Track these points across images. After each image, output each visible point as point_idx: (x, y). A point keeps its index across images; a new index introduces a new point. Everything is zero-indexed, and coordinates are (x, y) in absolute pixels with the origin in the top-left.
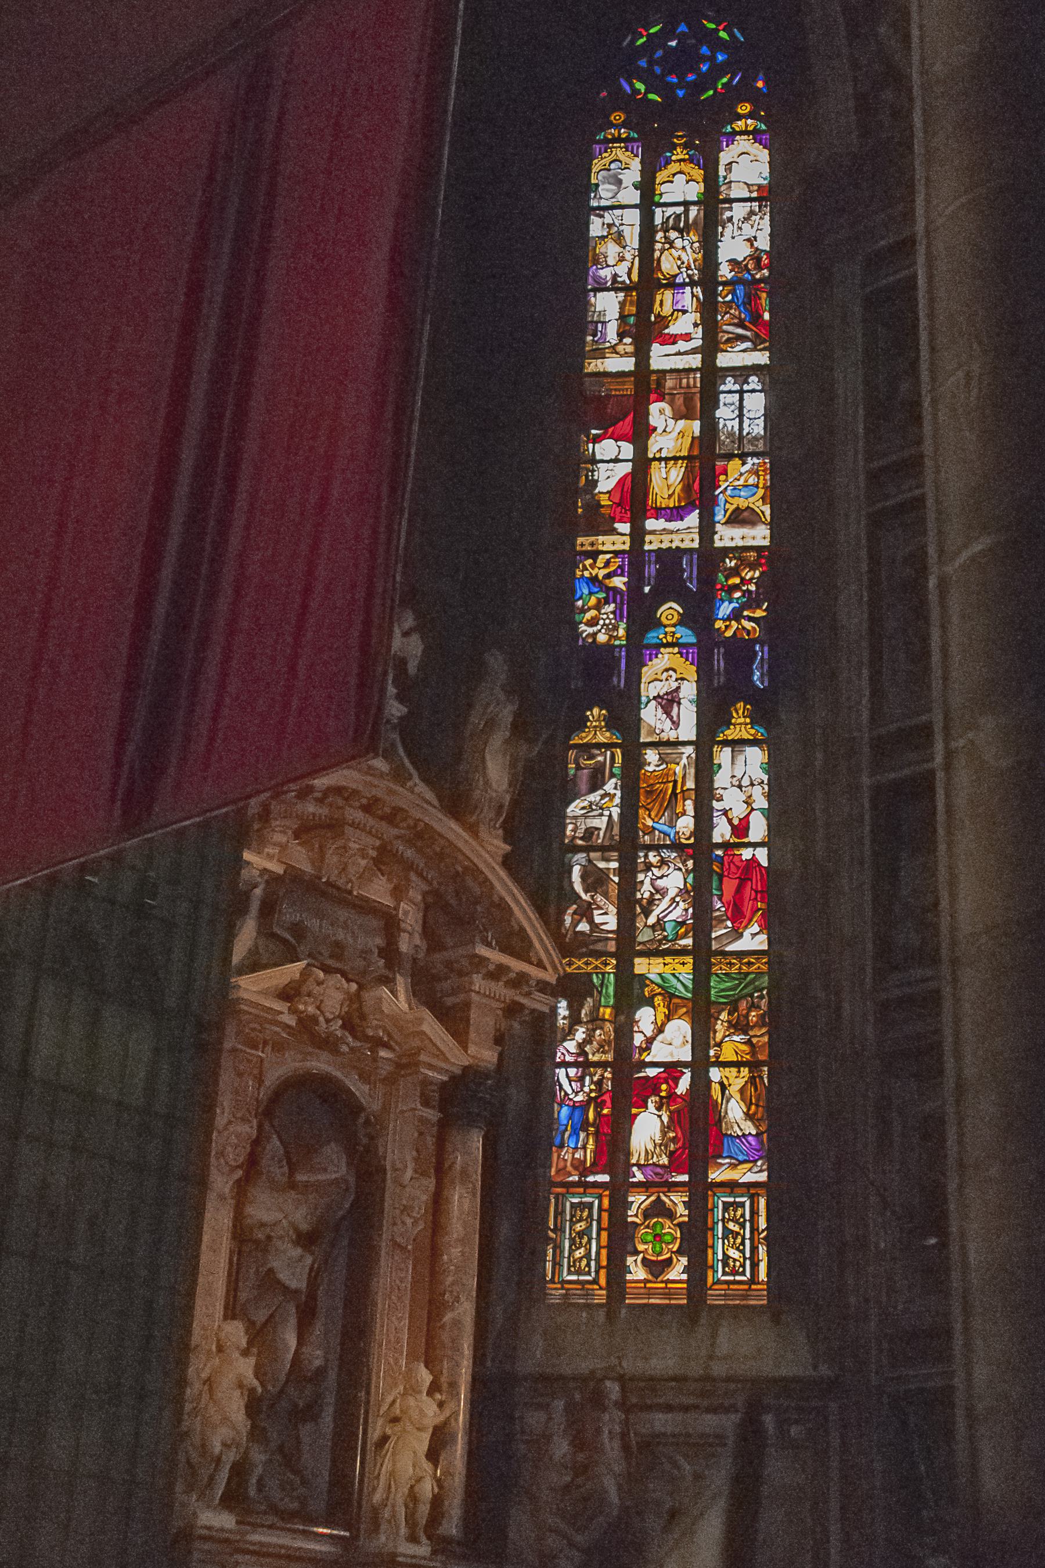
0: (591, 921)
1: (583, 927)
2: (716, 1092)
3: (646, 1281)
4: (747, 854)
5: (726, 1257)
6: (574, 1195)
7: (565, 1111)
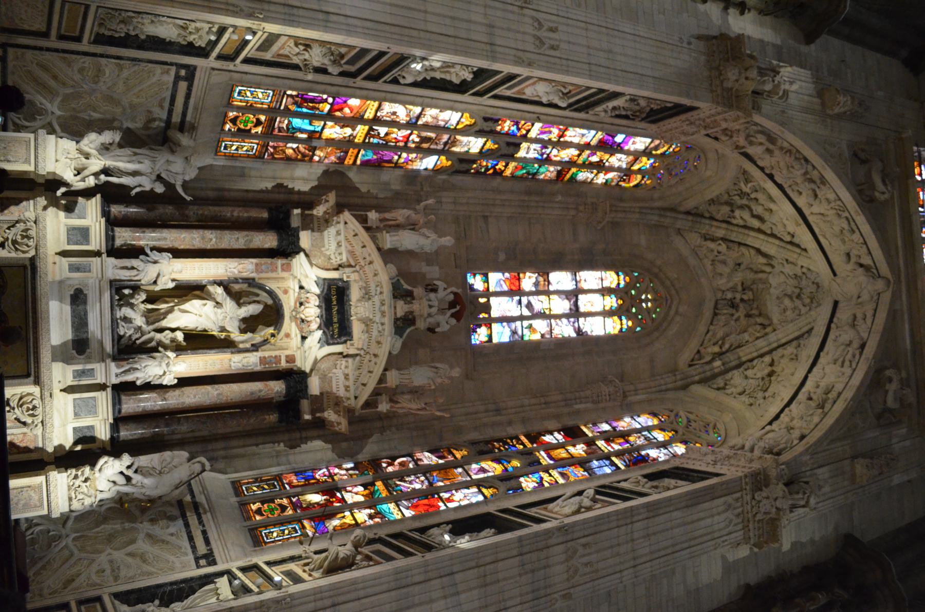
0: (387, 467)
1: (384, 465)
3: (252, 510)
4: (441, 504)
5: (272, 532)
7: (311, 474)
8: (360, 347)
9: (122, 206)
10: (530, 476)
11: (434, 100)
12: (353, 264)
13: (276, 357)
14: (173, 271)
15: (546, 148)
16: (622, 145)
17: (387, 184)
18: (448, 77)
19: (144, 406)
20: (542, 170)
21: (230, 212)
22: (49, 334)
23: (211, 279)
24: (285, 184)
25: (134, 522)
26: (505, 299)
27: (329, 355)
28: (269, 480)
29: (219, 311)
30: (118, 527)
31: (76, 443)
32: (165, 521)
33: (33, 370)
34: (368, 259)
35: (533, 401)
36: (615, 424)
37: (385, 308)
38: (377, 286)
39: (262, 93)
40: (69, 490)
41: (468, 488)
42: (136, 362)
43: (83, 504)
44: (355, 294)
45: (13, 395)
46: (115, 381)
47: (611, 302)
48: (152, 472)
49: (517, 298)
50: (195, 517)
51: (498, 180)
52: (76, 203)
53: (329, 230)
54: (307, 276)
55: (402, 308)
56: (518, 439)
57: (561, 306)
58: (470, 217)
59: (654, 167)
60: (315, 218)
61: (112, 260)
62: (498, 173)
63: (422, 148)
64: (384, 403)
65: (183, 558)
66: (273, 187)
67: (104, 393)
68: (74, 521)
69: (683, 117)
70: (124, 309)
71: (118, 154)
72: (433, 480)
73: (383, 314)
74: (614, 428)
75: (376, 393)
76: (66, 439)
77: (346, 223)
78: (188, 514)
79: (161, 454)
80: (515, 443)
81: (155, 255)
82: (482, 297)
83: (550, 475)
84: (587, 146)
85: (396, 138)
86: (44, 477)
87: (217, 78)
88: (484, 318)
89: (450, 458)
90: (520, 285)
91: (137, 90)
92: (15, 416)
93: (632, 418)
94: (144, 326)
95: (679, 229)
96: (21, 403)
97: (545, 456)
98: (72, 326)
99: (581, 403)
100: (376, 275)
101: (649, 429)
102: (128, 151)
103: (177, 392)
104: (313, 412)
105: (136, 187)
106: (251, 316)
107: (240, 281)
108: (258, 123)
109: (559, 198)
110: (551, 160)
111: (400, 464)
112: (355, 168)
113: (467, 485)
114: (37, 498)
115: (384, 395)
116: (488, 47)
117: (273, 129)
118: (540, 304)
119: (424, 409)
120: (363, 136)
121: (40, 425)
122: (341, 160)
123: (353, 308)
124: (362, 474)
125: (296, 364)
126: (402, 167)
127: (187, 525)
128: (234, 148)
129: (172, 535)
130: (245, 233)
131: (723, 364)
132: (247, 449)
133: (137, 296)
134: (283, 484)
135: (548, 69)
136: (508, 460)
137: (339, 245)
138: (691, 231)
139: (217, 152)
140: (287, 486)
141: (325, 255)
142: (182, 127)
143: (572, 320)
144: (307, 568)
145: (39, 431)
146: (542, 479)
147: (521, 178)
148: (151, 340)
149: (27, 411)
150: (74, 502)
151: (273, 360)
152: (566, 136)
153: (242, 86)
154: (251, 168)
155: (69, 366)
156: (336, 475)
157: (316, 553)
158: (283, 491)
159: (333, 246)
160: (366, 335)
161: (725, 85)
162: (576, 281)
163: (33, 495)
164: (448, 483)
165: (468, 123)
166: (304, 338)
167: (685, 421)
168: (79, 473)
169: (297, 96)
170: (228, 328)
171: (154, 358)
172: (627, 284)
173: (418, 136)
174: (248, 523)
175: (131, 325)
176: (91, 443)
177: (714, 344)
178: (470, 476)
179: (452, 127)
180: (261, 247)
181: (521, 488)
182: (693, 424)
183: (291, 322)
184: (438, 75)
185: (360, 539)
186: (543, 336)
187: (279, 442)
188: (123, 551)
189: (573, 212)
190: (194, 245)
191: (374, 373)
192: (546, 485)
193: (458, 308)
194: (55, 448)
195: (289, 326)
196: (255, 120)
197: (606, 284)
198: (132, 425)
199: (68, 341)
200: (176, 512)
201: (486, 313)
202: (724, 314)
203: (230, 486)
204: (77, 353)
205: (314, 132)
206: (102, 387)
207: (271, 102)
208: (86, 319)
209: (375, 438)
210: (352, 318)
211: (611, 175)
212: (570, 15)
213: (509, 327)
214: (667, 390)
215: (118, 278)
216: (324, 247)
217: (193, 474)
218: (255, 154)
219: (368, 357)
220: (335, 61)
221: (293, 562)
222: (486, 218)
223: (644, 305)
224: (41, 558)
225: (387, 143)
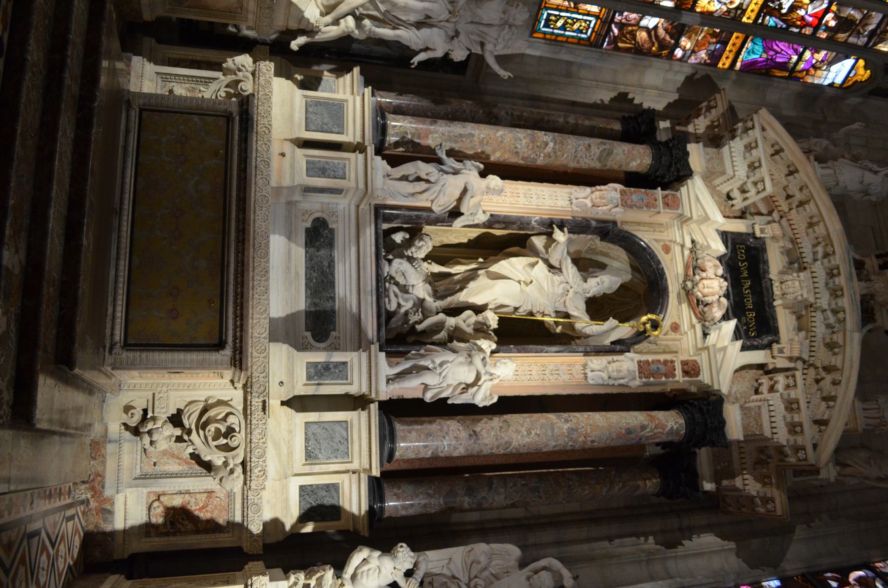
8: (796, 354)
12: (764, 211)
13: (666, 362)
22: (267, 280)
23: (547, 217)
24: (630, 96)
29: (557, 278)
31: (304, 518)
34: (799, 196)
37: (841, 281)
38: (814, 246)
42: (422, 356)
44: (775, 261)
45: (191, 403)
46: (386, 392)
54: (706, 219)
61: (380, 164)
66: (612, 100)
67: (364, 414)
70: (397, 262)
73: (836, 293)
76: (287, 507)
77: (763, 129)
79: (469, 547)
81: (451, 162)
92: (190, 450)
94: (429, 300)
96: (204, 419)
98: (306, 284)
100: (811, 225)
103: (496, 421)
104: (717, 478)
107: (594, 223)
120: (756, 9)
121: (239, 470)
122: (715, 57)
123: (776, 284)
125: (700, 378)
126: (798, 79)
128: (559, 24)
132: (594, 545)
133: (418, 243)
137: (753, 167)
139: (534, 30)
145: (236, 483)
148: (439, 326)
149: (214, 439)
151: (663, 369)
154: (581, 66)
155: (301, 354)
159: (742, 171)
160: (803, 334)
171: (454, 351)
173: (837, 17)
175: (406, 296)
176: (332, 520)
183: (680, 303)
187: (646, 535)
191: (839, 400)
194: (265, 524)
198: (408, 489)
199: (298, 313)
204: (314, 337)
206: (358, 402)
208: (333, 274)
215: (390, 202)
216: (723, 173)
218: (589, 38)
225: (789, 26)
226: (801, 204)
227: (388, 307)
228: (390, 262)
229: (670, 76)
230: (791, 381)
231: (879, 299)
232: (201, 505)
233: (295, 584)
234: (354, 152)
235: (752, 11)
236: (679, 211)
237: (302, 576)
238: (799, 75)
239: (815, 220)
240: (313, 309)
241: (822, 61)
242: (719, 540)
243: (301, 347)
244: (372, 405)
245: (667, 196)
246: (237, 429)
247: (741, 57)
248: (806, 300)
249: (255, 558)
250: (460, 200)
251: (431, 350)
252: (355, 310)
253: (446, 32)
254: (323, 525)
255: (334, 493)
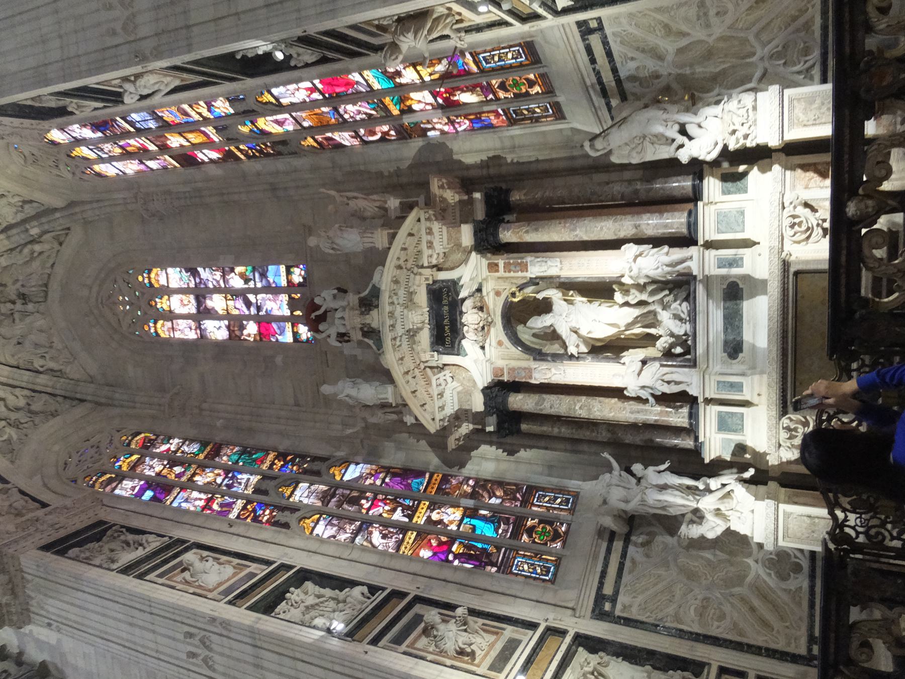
0: (389, 131)
1: (392, 133)
2: (436, 76)
3: (539, 85)
4: (320, 86)
5: (513, 58)
6: (512, 117)
7: (474, 125)
8: (418, 277)
9: (682, 446)
10: (224, 114)
11: (338, 556)
12: (428, 369)
13: (509, 271)
14: (623, 377)
15: (227, 485)
16: (147, 486)
17: (399, 449)
18: (318, 590)
19: (660, 219)
20: (235, 457)
21: (565, 431)
22: (769, 315)
23: (581, 362)
24: (506, 454)
25: (679, 75)
26: (276, 312)
27: (452, 269)
28: (523, 120)
29: (574, 324)
30: (699, 69)
31: (745, 174)
32: (641, 75)
33: (791, 280)
34: (409, 377)
35: (236, 197)
36: (142, 167)
37: (389, 322)
38: (400, 346)
39: (523, 571)
40: (755, 120)
41: (292, 104)
42: (668, 273)
43: (740, 101)
44: (425, 337)
46: (693, 251)
47: (163, 304)
48: (655, 139)
49: (262, 313)
50: (604, 81)
51: (281, 449)
52: (733, 454)
53: (452, 412)
54: (475, 361)
55: (374, 319)
56: (246, 155)
57: (217, 302)
58: (313, 407)
59: (115, 457)
60: (471, 418)
61: (693, 391)
62: (281, 456)
63: (359, 491)
64: (392, 208)
65: (619, 30)
66: (518, 451)
67: (707, 238)
68: (753, 76)
69: (62, 533)
71: (683, 508)
72: (334, 114)
73: (392, 314)
74: (142, 163)
75: (402, 218)
77: (433, 419)
78: (613, 84)
79: (642, 161)
80: (250, 151)
81: (644, 394)
82: (298, 316)
83: (200, 114)
84: (183, 489)
85: (386, 504)
86: (785, 139)
87: (569, 596)
88: (296, 294)
89: (319, 138)
90: (259, 327)
91: (660, 586)
92: (817, 215)
93: (124, 173)
95: (92, 382)
96: (809, 233)
97: (212, 136)
99: (185, 193)
100: (402, 359)
101: (101, 160)
102: (673, 512)
103: (622, 235)
104: (471, 201)
105: (663, 471)
106: (540, 315)
107: (549, 358)
108: (530, 531)
109: (219, 423)
110: (224, 470)
111: (374, 133)
112: (432, 469)
113: (293, 107)
114: (796, 111)
115: (393, 217)
116: (259, 644)
117: (514, 523)
118: (238, 307)
119: (348, 198)
120: (420, 509)
121: (786, 205)
123: (427, 321)
124: (417, 124)
125: (487, 262)
127: (615, 70)
128: (559, 500)
129: (632, 59)
130: (544, 412)
131: (27, 230)
133: (667, 345)
134: (505, 114)
135: (194, 614)
136: (253, 134)
137: (441, 395)
138: (78, 381)
140: (501, 112)
141: (459, 381)
142: (612, 536)
143: (202, 286)
144: (457, 17)
146: (209, 110)
147: (258, 450)
148: (652, 293)
150: (750, 106)
151: (512, 268)
152: (206, 500)
153: (544, 580)
154: (541, 474)
156: (446, 124)
157: (447, 37)
158: (505, 107)
159: (447, 395)
161: (7, 577)
162: (200, 329)
163: (801, 115)
164: (317, 111)
165: (307, 521)
166: (479, 290)
167: (61, 167)
168: (742, 142)
169: (487, 564)
170: (565, 303)
171: (647, 276)
172: (147, 323)
173: (361, 506)
174: (542, 71)
175: (675, 312)
177: (41, 253)
178: (292, 116)
179: (324, 516)
180: (527, 395)
181: (229, 101)
182: (52, 164)
184: (328, 592)
185: (391, 56)
186: (232, 270)
187: (512, 163)
188: (692, 40)
189: (205, 406)
190: (600, 402)
191: (399, 248)
192: (202, 103)
193: (313, 316)
194: (770, 170)
195: (496, 305)
196: (534, 536)
197: (169, 324)
198: (677, 193)
199: (747, 300)
200: (627, 86)
201: (294, 298)
202: (33, 286)
203: (567, 116)
204: (738, 285)
205: (471, 517)
206: (709, 245)
207: (515, 558)
208: (725, 324)
209: (407, 163)
210: (428, 309)
211: (164, 448)
212: (176, 668)
213: (268, 281)
214: (91, 202)
215: (686, 370)
216: (458, 393)
217: (605, 136)
219: (409, 266)
220: (432, 628)
221: (478, 25)
222: (297, 404)
223: (127, 299)
224: (798, 30)
225: (395, 499)
226: (407, 373)
227: (688, 305)
228: (686, 334)
229: (477, 468)
230: (430, 260)
231: (357, 312)
232: (812, 180)
233: (752, 140)
234: (712, 399)
235: (423, 508)
236: (493, 366)
237: (748, 145)
238: (382, 470)
239: (400, 362)
240: (738, 302)
241: (367, 478)
242: (463, 160)
243: (747, 278)
244: (702, 243)
245: (501, 376)
246: (788, 227)
247: (426, 480)
248: (409, 311)
249: (777, 150)
250: (641, 370)
251: (663, 277)
252: (711, 302)
253: (647, 481)
254: (733, 170)
255: (725, 189)
